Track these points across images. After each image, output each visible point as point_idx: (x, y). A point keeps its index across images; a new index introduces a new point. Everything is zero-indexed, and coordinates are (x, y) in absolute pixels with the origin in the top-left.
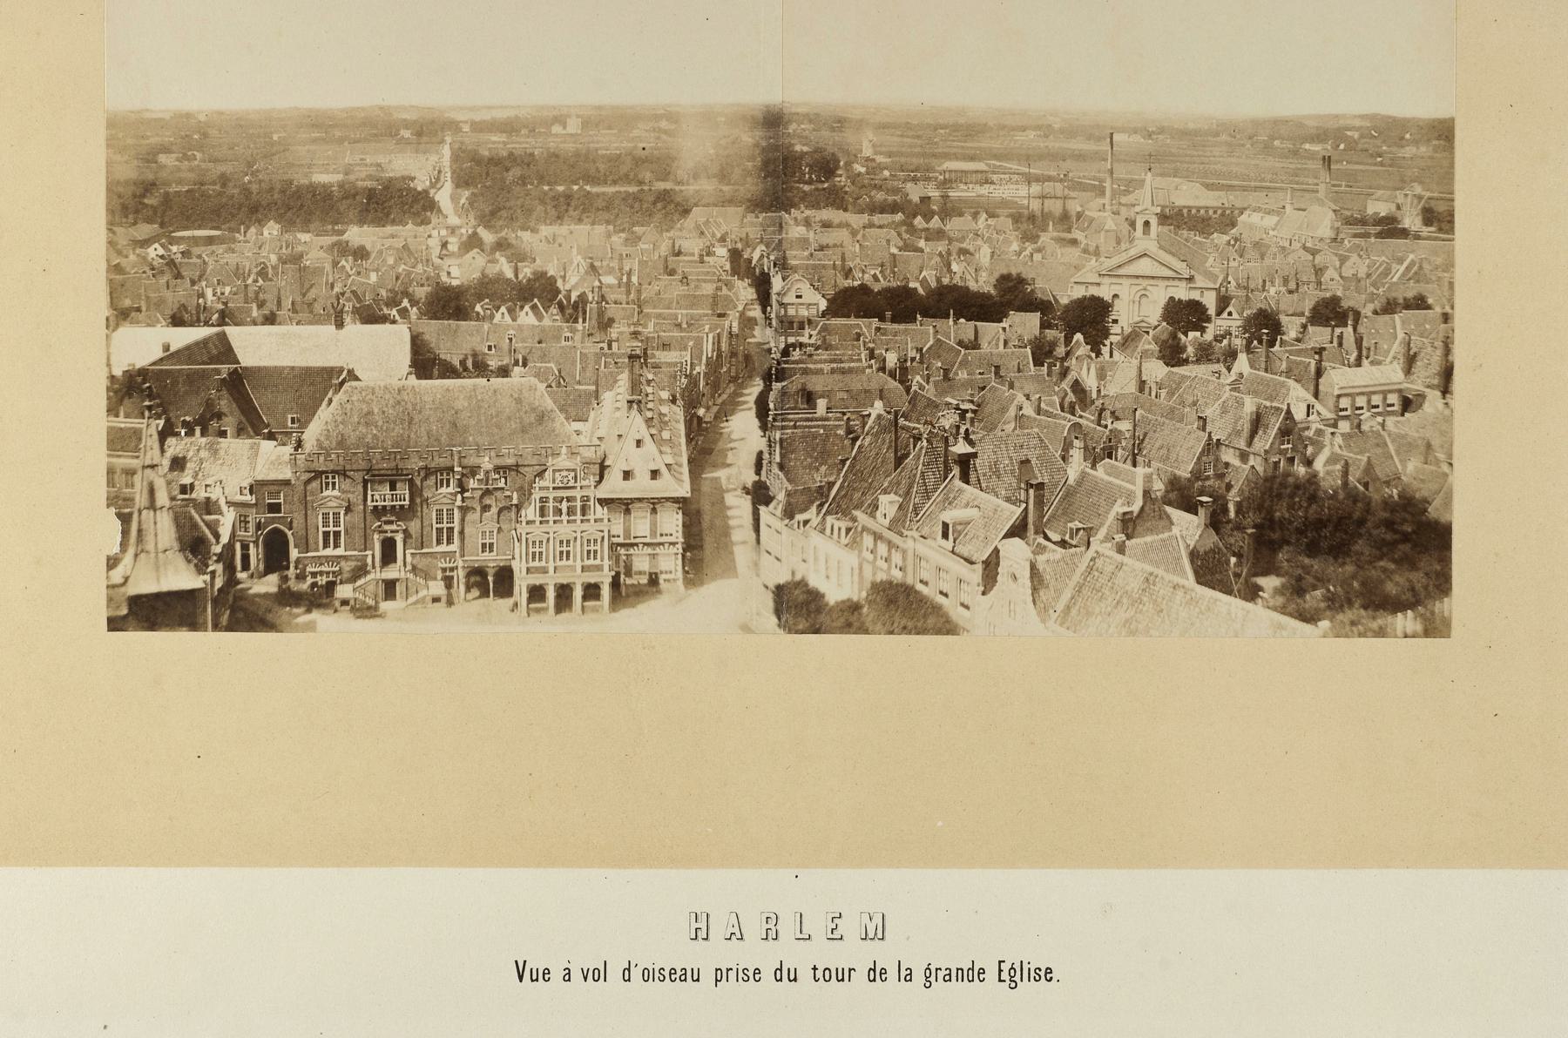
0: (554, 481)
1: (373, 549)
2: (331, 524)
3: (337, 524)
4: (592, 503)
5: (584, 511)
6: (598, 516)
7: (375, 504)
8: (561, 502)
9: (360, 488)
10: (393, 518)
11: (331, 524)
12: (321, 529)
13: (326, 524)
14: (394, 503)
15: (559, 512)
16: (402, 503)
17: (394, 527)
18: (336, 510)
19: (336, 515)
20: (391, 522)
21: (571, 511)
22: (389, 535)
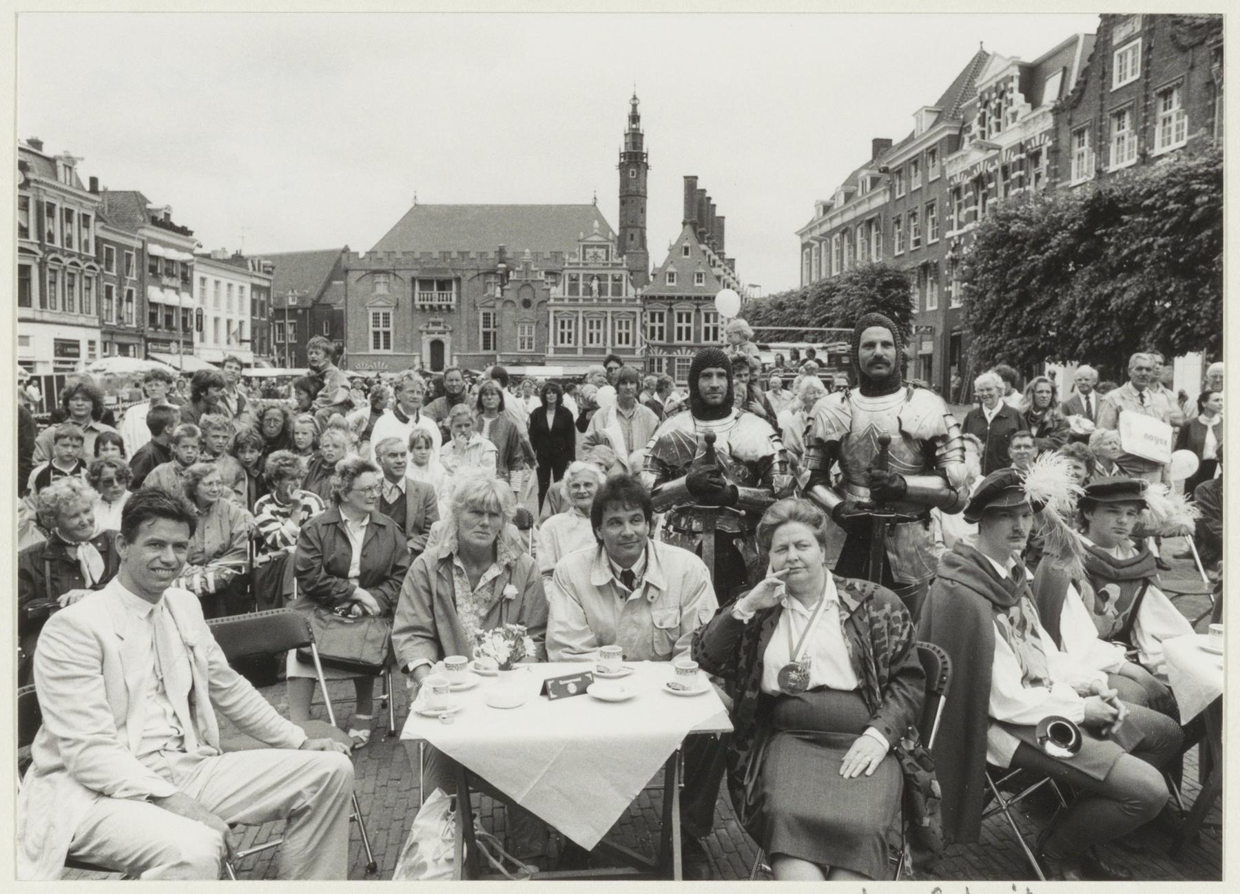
0: (584, 258)
1: (421, 351)
2: (381, 324)
3: (387, 324)
4: (624, 282)
5: (617, 290)
6: (631, 296)
7: (422, 302)
8: (592, 279)
9: (409, 289)
10: (440, 319)
11: (381, 324)
12: (371, 329)
13: (376, 324)
14: (441, 303)
15: (589, 290)
16: (448, 303)
17: (441, 328)
18: (386, 310)
19: (386, 316)
20: (438, 324)
21: (602, 291)
22: (436, 336)
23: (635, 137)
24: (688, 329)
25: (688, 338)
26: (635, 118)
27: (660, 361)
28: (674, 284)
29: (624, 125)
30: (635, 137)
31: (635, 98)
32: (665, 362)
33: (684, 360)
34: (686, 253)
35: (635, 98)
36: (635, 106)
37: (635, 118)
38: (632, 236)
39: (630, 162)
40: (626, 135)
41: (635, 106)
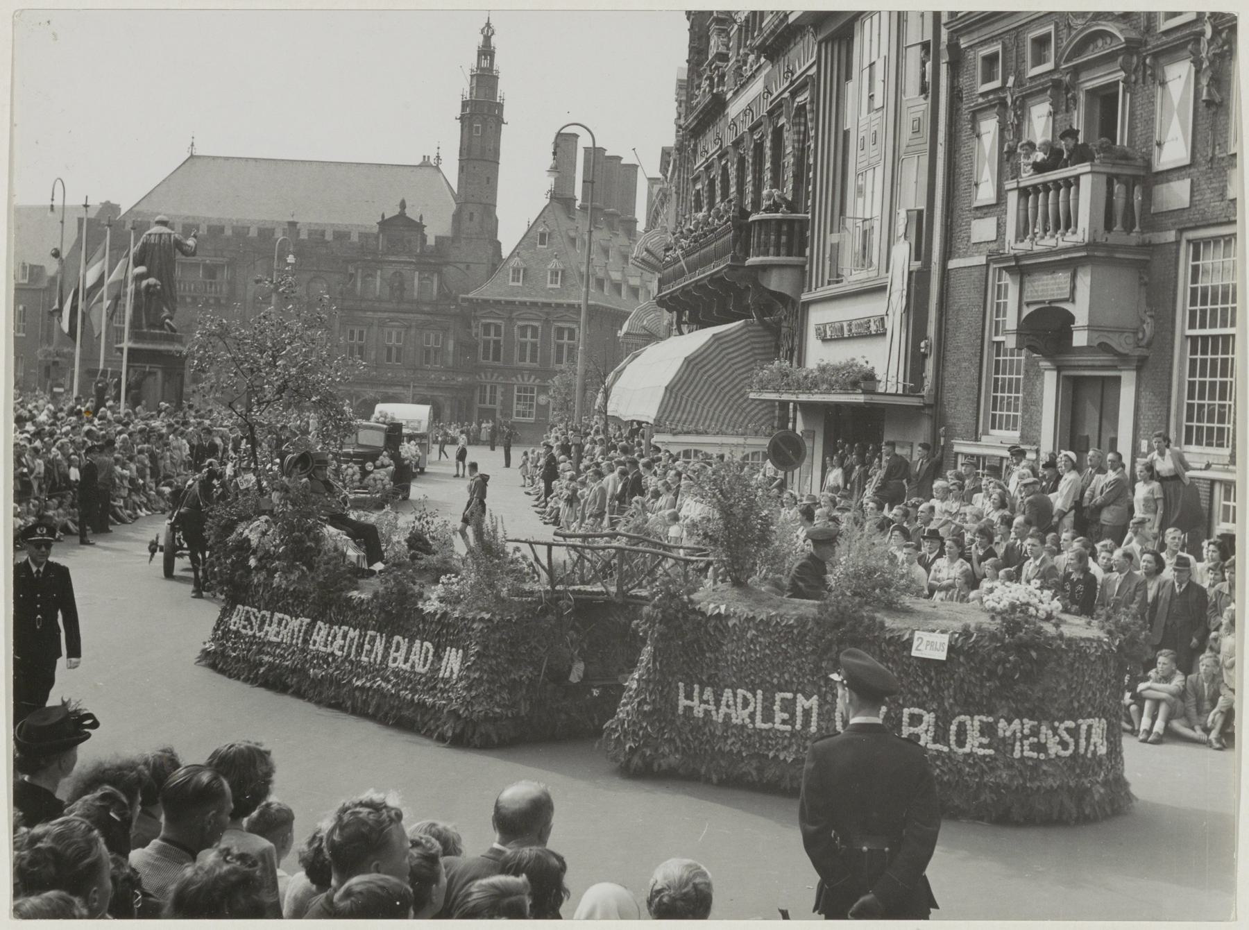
23: (485, 79)
24: (534, 345)
25: (533, 359)
26: (486, 51)
27: (493, 389)
28: (520, 284)
29: (471, 60)
30: (485, 79)
31: (488, 25)
32: (500, 390)
33: (526, 390)
34: (542, 242)
35: (488, 25)
36: (487, 39)
37: (486, 51)
38: (472, 214)
39: (471, 114)
40: (472, 76)
41: (487, 39)
